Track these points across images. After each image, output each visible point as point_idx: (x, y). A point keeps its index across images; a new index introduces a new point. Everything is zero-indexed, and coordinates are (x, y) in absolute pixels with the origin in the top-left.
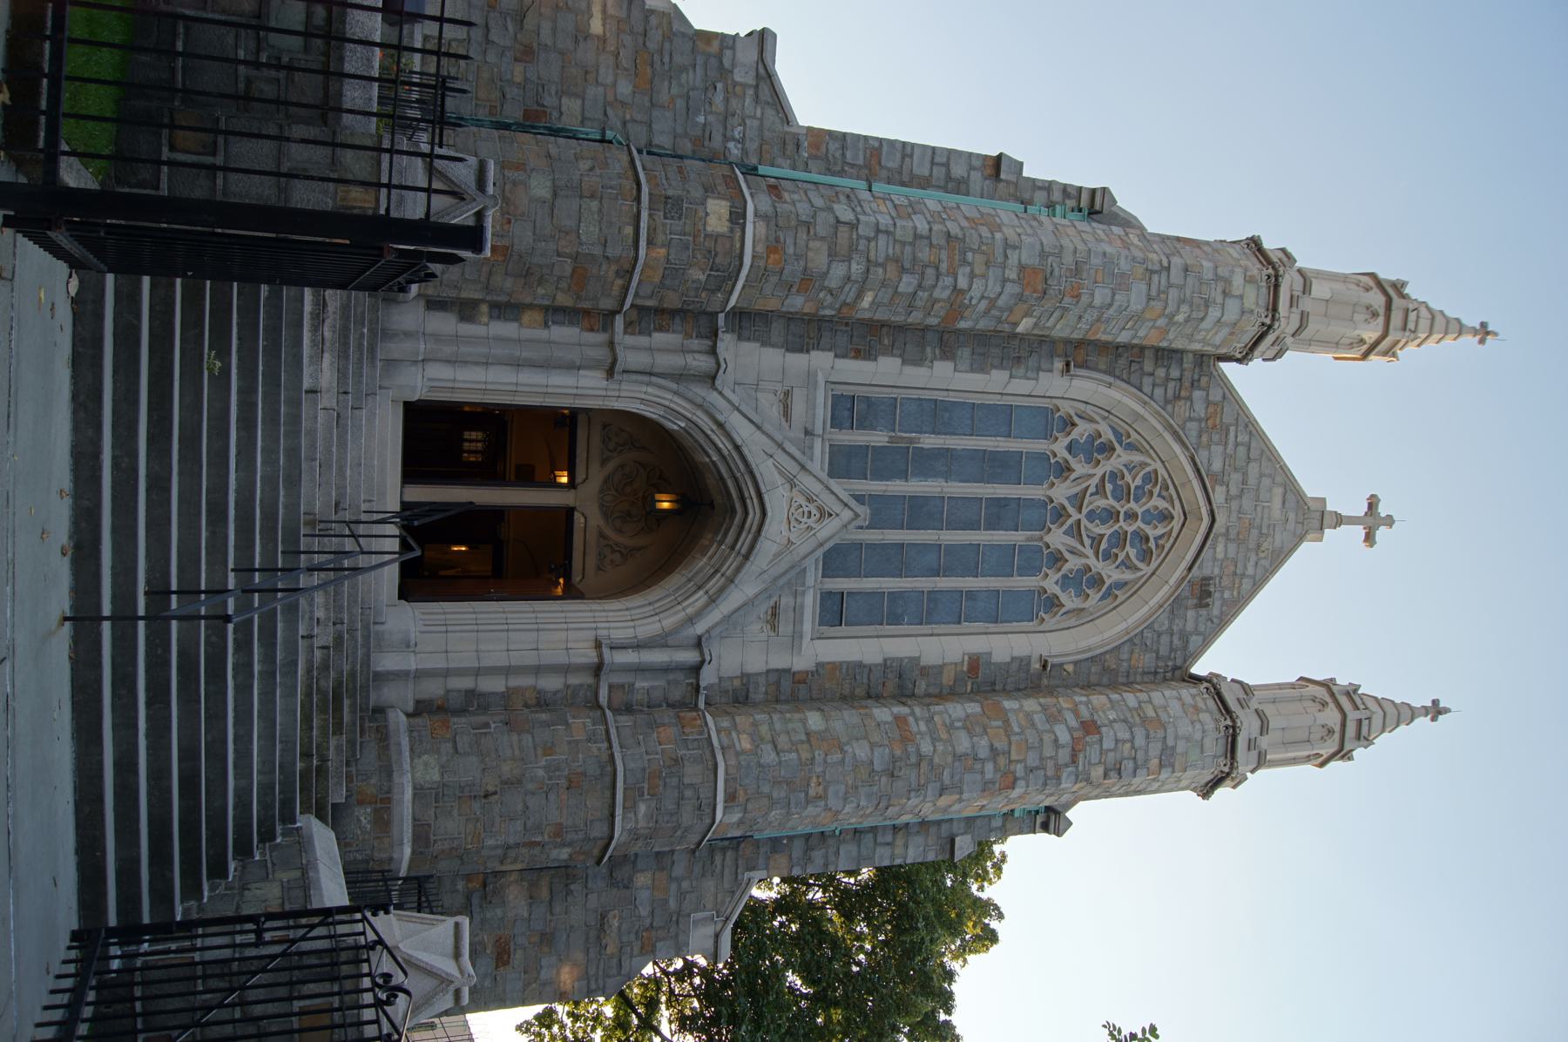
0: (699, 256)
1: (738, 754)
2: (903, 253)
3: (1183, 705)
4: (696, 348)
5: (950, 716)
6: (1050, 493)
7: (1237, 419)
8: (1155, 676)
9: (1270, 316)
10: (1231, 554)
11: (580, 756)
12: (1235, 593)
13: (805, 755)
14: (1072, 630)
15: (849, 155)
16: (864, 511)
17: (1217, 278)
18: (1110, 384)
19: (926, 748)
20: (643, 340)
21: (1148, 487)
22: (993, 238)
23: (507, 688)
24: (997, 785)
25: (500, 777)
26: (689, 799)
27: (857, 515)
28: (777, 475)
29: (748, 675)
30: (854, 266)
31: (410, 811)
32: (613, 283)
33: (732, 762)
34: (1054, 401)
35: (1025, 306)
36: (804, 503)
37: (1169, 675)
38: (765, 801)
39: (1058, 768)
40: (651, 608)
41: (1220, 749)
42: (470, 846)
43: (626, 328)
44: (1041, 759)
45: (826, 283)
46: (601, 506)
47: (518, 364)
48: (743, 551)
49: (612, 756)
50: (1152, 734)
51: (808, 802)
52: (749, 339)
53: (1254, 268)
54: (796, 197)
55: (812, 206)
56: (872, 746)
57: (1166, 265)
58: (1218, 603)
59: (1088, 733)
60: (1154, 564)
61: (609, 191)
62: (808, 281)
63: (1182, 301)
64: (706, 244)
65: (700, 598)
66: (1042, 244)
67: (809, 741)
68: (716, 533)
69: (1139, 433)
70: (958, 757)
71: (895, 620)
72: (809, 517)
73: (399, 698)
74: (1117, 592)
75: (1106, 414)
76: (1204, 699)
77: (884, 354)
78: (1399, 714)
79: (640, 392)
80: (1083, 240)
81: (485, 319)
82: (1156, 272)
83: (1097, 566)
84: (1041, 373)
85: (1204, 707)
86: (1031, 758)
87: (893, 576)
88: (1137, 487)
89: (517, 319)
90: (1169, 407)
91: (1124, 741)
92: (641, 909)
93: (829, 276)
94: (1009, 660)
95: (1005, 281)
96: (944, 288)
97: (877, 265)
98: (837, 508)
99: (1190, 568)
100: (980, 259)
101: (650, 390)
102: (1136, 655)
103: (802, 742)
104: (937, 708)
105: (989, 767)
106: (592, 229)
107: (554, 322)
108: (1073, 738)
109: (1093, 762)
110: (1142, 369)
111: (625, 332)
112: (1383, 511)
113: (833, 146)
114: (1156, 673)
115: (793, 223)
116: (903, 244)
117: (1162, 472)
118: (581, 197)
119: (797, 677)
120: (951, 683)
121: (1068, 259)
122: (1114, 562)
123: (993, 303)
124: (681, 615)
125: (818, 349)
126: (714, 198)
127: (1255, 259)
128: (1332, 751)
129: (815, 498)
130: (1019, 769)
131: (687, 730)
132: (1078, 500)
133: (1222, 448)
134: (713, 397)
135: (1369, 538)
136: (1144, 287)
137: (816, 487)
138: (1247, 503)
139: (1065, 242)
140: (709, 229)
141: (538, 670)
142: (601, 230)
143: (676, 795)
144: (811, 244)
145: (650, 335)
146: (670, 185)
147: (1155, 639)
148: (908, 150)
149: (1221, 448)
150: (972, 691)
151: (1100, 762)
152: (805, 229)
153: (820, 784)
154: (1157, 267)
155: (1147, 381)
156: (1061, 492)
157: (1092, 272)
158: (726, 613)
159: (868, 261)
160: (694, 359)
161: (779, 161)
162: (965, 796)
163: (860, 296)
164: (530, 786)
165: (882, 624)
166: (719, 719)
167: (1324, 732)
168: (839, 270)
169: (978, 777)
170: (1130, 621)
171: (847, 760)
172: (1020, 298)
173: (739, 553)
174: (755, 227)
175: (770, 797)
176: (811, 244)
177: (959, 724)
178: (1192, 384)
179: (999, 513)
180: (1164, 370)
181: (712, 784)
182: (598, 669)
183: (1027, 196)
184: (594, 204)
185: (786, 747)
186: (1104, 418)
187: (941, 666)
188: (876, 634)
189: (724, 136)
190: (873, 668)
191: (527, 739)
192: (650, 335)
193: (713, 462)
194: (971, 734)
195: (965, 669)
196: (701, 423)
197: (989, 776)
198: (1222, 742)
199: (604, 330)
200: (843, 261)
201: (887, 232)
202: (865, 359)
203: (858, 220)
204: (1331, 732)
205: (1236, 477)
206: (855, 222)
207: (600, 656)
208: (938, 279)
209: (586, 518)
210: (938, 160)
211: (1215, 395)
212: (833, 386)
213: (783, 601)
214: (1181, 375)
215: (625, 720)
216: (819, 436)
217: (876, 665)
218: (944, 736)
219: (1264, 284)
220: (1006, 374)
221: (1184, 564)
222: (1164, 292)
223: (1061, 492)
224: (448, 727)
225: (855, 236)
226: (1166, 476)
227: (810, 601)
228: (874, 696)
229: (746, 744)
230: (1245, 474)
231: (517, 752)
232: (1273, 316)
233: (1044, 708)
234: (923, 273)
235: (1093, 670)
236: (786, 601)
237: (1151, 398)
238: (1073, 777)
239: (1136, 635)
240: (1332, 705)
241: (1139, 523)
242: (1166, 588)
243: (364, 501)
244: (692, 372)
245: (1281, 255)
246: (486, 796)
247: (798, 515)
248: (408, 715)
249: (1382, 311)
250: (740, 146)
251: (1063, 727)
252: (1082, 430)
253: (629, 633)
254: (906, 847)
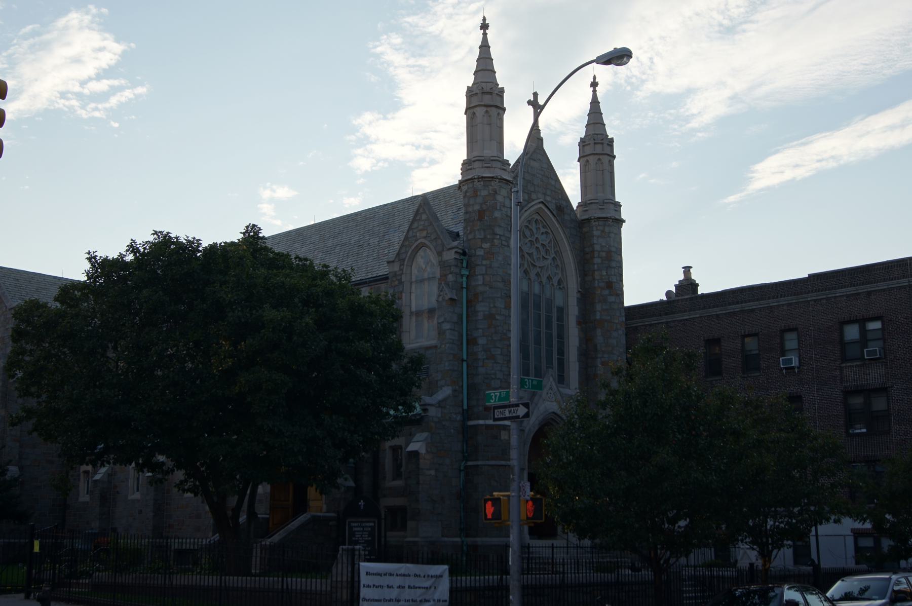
17: (500, 210)
60: (550, 231)
76: (599, 225)
232: (511, 183)
240: (601, 157)
242: (559, 229)
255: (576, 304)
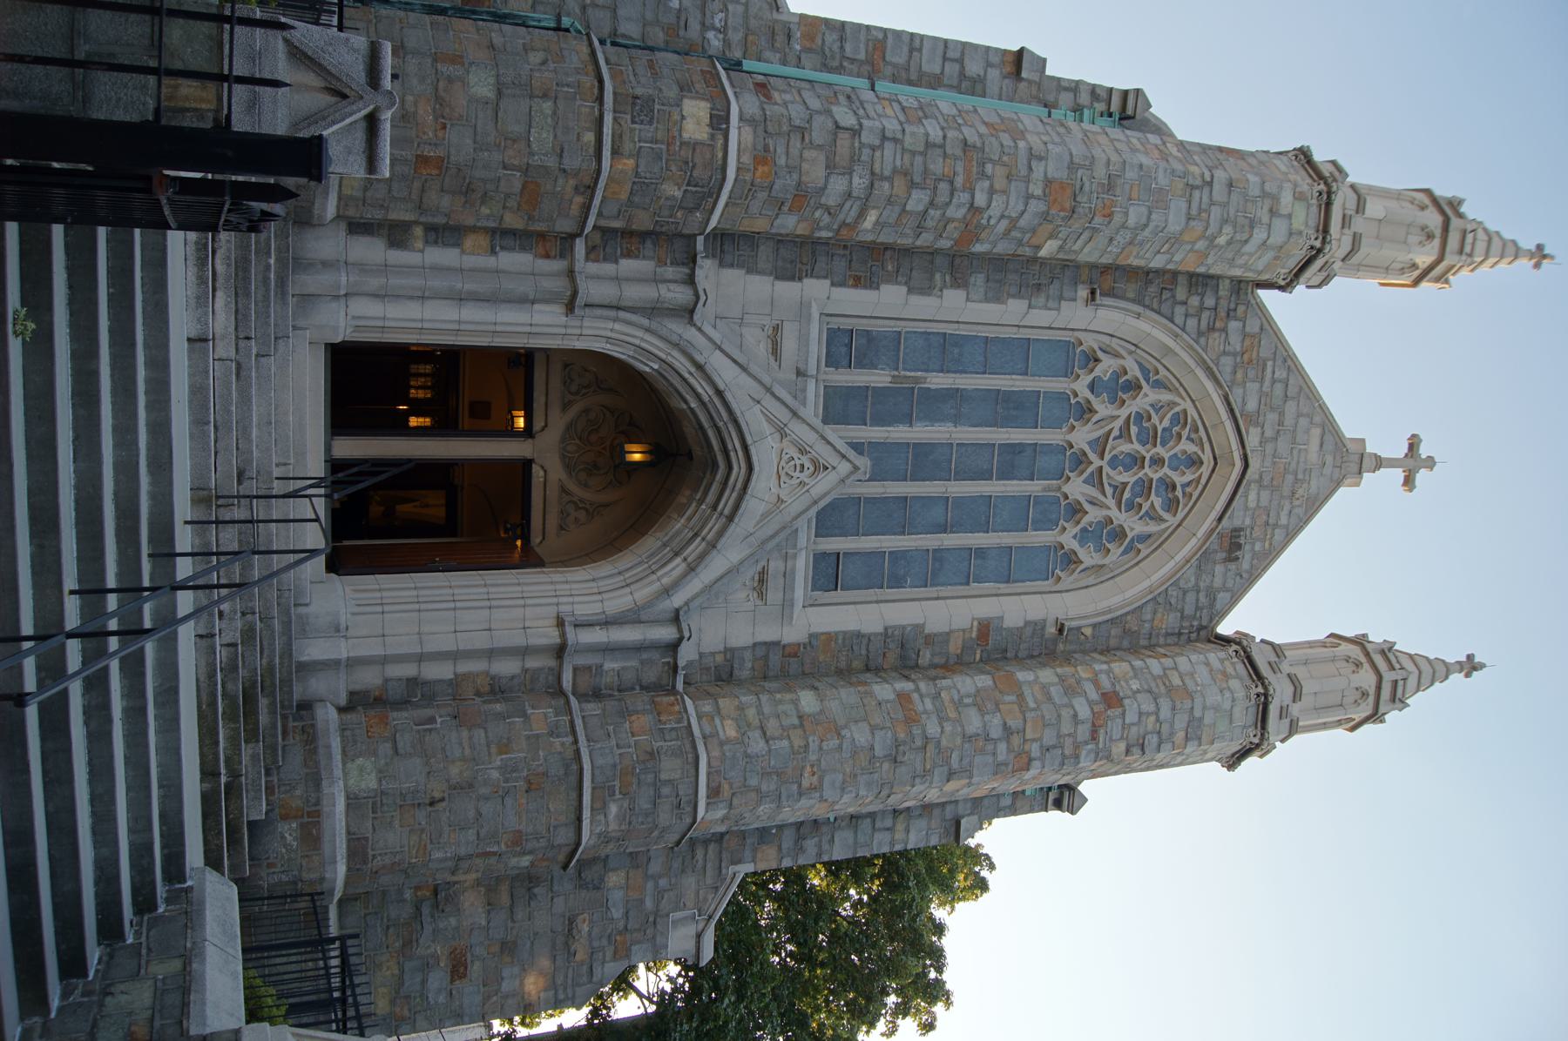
0: (673, 168)
1: (722, 744)
2: (912, 165)
3: (1211, 670)
4: (671, 277)
5: (959, 692)
6: (1069, 437)
7: (1275, 353)
8: (1179, 638)
9: (1321, 237)
10: (1264, 502)
11: (541, 753)
12: (1267, 545)
13: (798, 742)
14: (1091, 589)
15: (848, 47)
16: (864, 463)
18: (1139, 314)
19: (933, 729)
20: (608, 268)
21: (1176, 429)
22: (1016, 147)
23: (455, 674)
24: (1010, 767)
25: (448, 781)
26: (667, 797)
27: (856, 468)
28: (765, 424)
29: (732, 650)
30: (856, 180)
31: (344, 823)
32: (571, 201)
33: (716, 753)
34: (1076, 333)
35: (1051, 226)
36: (796, 455)
37: (1194, 636)
38: (753, 795)
39: (1077, 746)
40: (622, 578)
41: (1251, 719)
42: (414, 860)
43: (587, 254)
44: (1059, 736)
45: (823, 200)
46: (563, 457)
47: (461, 298)
48: (726, 512)
49: (578, 752)
50: (1178, 705)
51: (800, 794)
52: (732, 266)
53: (1304, 182)
54: (788, 97)
55: (808, 108)
56: (873, 729)
57: (1209, 179)
58: (1248, 556)
59: (1110, 707)
60: (1180, 515)
61: (566, 89)
62: (802, 198)
63: (1225, 221)
64: (682, 153)
65: (677, 565)
66: (1071, 154)
67: (802, 725)
68: (696, 490)
69: (1168, 370)
70: (968, 738)
71: (897, 582)
72: (802, 471)
73: (329, 689)
74: (1139, 546)
75: (1133, 348)
76: (1233, 664)
77: (888, 282)
78: (1434, 672)
79: (605, 329)
80: (1117, 150)
81: (419, 245)
82: (1197, 187)
83: (1120, 517)
84: (1062, 302)
85: (1233, 673)
86: (1049, 737)
87: (895, 534)
88: (1164, 430)
89: (457, 245)
90: (1202, 340)
91: (1148, 714)
92: (613, 910)
93: (827, 192)
94: (1021, 624)
95: (1029, 197)
96: (959, 206)
97: (883, 178)
98: (833, 459)
99: (1220, 519)
100: (1000, 172)
101: (617, 326)
102: (1159, 615)
103: (795, 727)
104: (945, 683)
105: (1002, 747)
106: (545, 135)
107: (502, 248)
108: (1094, 713)
109: (1114, 738)
110: (1174, 297)
111: (587, 259)
112: (1424, 451)
113: (831, 38)
114: (1180, 634)
115: (785, 128)
116: (913, 153)
117: (1192, 412)
118: (531, 97)
119: (787, 650)
120: (959, 651)
121: (1100, 172)
122: (1138, 514)
123: (1014, 222)
124: (656, 586)
125: (811, 276)
126: (692, 98)
127: (1304, 173)
128: (1364, 715)
129: (808, 449)
130: (1035, 749)
131: (663, 718)
132: (1100, 446)
133: (1258, 385)
134: (691, 334)
135: (1409, 482)
136: (1184, 205)
137: (809, 437)
138: (1283, 445)
139: (1097, 152)
140: (686, 136)
141: (491, 654)
142: (555, 136)
143: (652, 793)
144: (806, 154)
145: (616, 262)
146: (638, 82)
147: (1181, 596)
148: (917, 43)
149: (1256, 386)
150: (981, 660)
151: (1122, 738)
152: (799, 136)
153: (813, 775)
154: (1198, 182)
155: (1180, 310)
156: (1082, 437)
157: (1127, 187)
158: (707, 582)
159: (873, 173)
160: (669, 290)
161: (768, 54)
162: (975, 780)
163: (862, 215)
164: (483, 791)
165: (882, 588)
166: (701, 702)
167: (1358, 695)
168: (838, 185)
169: (990, 759)
170: (1155, 577)
171: (844, 747)
172: (1045, 217)
173: (721, 514)
174: (739, 134)
175: (758, 790)
176: (806, 154)
177: (966, 701)
178: (1228, 314)
179: (1013, 461)
180: (1199, 298)
181: (693, 779)
182: (560, 651)
183: (1051, 98)
184: (547, 106)
185: (776, 734)
186: (1131, 353)
187: (948, 634)
188: (875, 598)
189: (703, 24)
190: (872, 638)
191: (479, 734)
192: (616, 262)
193: (692, 410)
194: (982, 712)
195: (974, 635)
196: (677, 365)
197: (1001, 758)
198: (1252, 711)
199: (562, 256)
200: (844, 174)
201: (895, 140)
202: (865, 287)
203: (861, 125)
204: (1365, 694)
205: (1272, 417)
206: (857, 127)
207: (563, 635)
208: (952, 194)
209: (545, 471)
210: (950, 54)
211: (1253, 326)
212: (829, 319)
213: (772, 564)
214: (1217, 304)
215: (593, 708)
216: (812, 376)
217: (876, 635)
218: (952, 715)
219: (1314, 201)
220: (1023, 304)
221: (1214, 515)
222: (1205, 211)
223: (1082, 437)
224: (387, 724)
225: (857, 145)
226: (1196, 417)
227: (802, 565)
228: (872, 668)
229: (730, 731)
230: (1282, 414)
231: (467, 752)
232: (1324, 238)
233: (1062, 679)
234: (935, 188)
235: (1113, 632)
236: (776, 565)
237: (1183, 330)
238: (1093, 756)
239: (1160, 594)
240: (1366, 666)
241: (1166, 470)
242: (1194, 541)
243: (277, 465)
244: (666, 305)
245: (1331, 168)
246: (432, 804)
247: (789, 468)
248: (341, 710)
249: (1438, 232)
250: (721, 36)
251: (1084, 702)
252: (1106, 367)
253: (597, 608)
254: (907, 831)
255: (1031, 616)
